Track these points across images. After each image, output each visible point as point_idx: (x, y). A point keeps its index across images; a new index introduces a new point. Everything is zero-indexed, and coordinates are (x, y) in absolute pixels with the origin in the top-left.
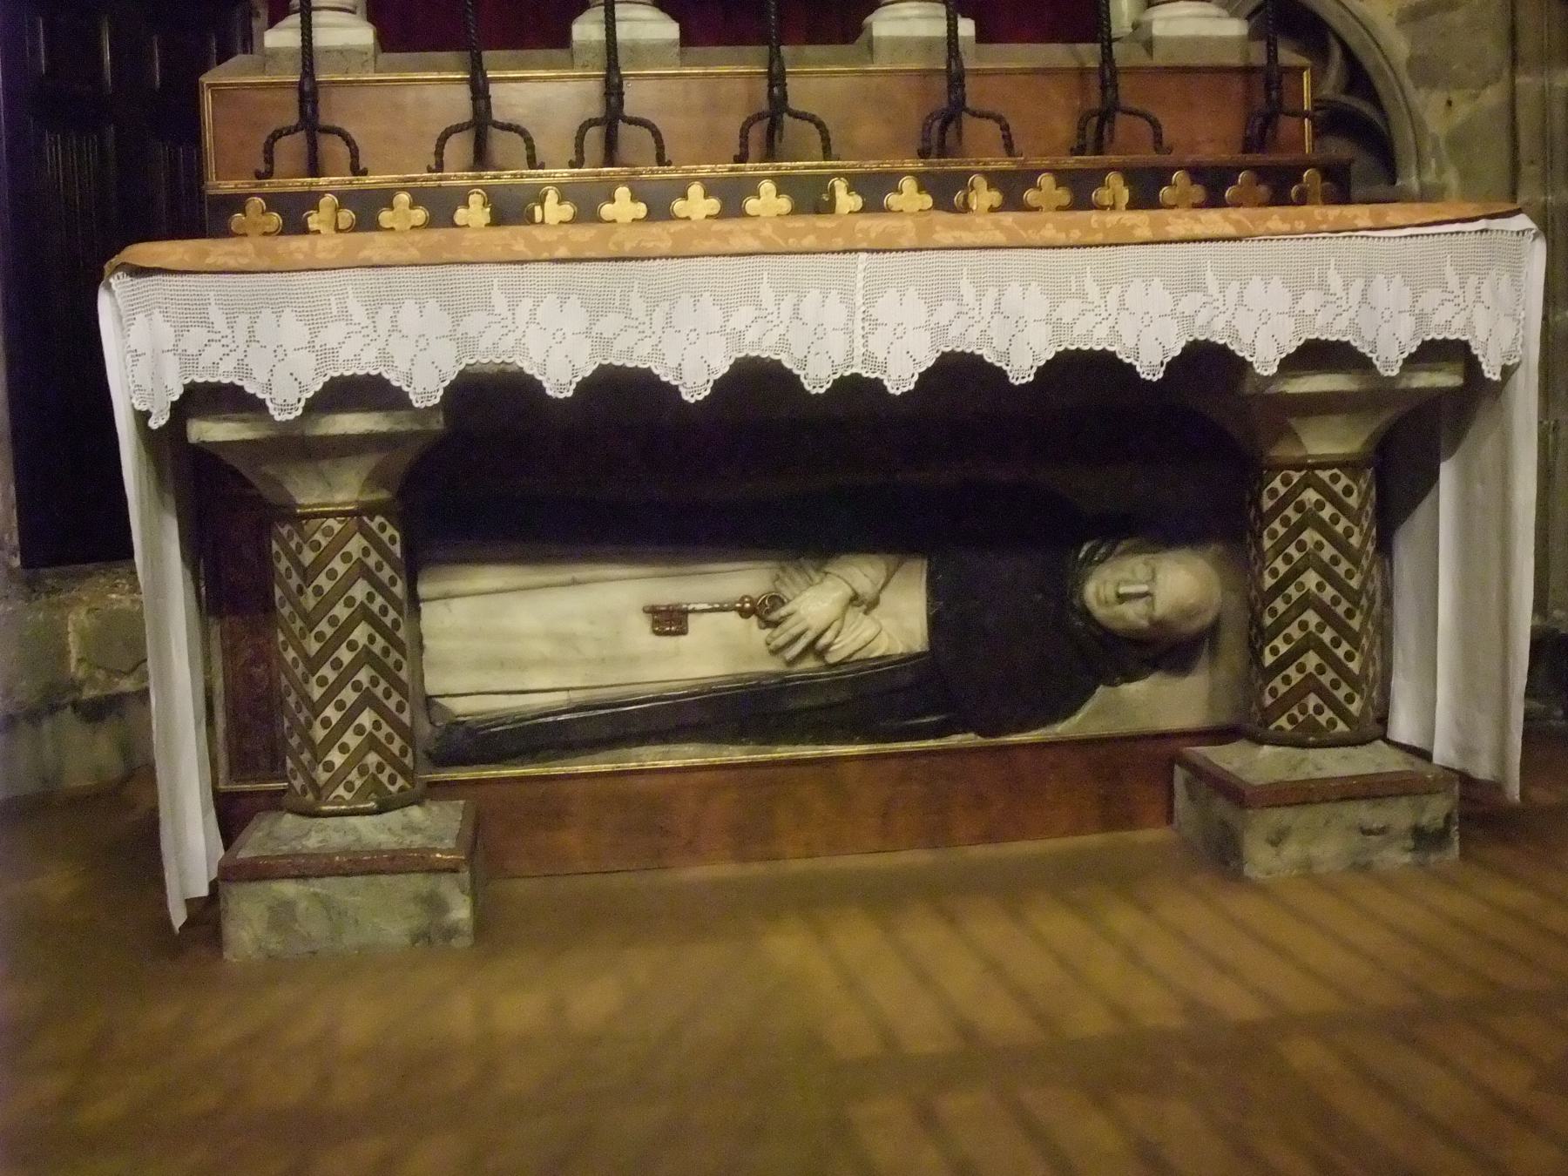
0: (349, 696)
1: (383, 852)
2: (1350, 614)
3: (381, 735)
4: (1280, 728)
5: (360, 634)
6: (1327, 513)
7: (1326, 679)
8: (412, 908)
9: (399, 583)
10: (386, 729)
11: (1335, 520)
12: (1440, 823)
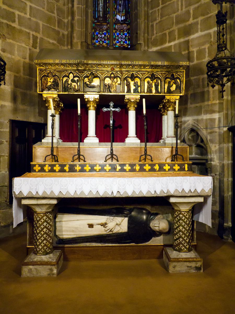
0: (42, 238)
1: (45, 262)
2: (187, 233)
3: (47, 244)
4: (176, 249)
5: (45, 230)
6: (183, 218)
7: (183, 242)
8: (48, 271)
9: (51, 222)
10: (48, 243)
11: (185, 219)
12: (200, 266)
